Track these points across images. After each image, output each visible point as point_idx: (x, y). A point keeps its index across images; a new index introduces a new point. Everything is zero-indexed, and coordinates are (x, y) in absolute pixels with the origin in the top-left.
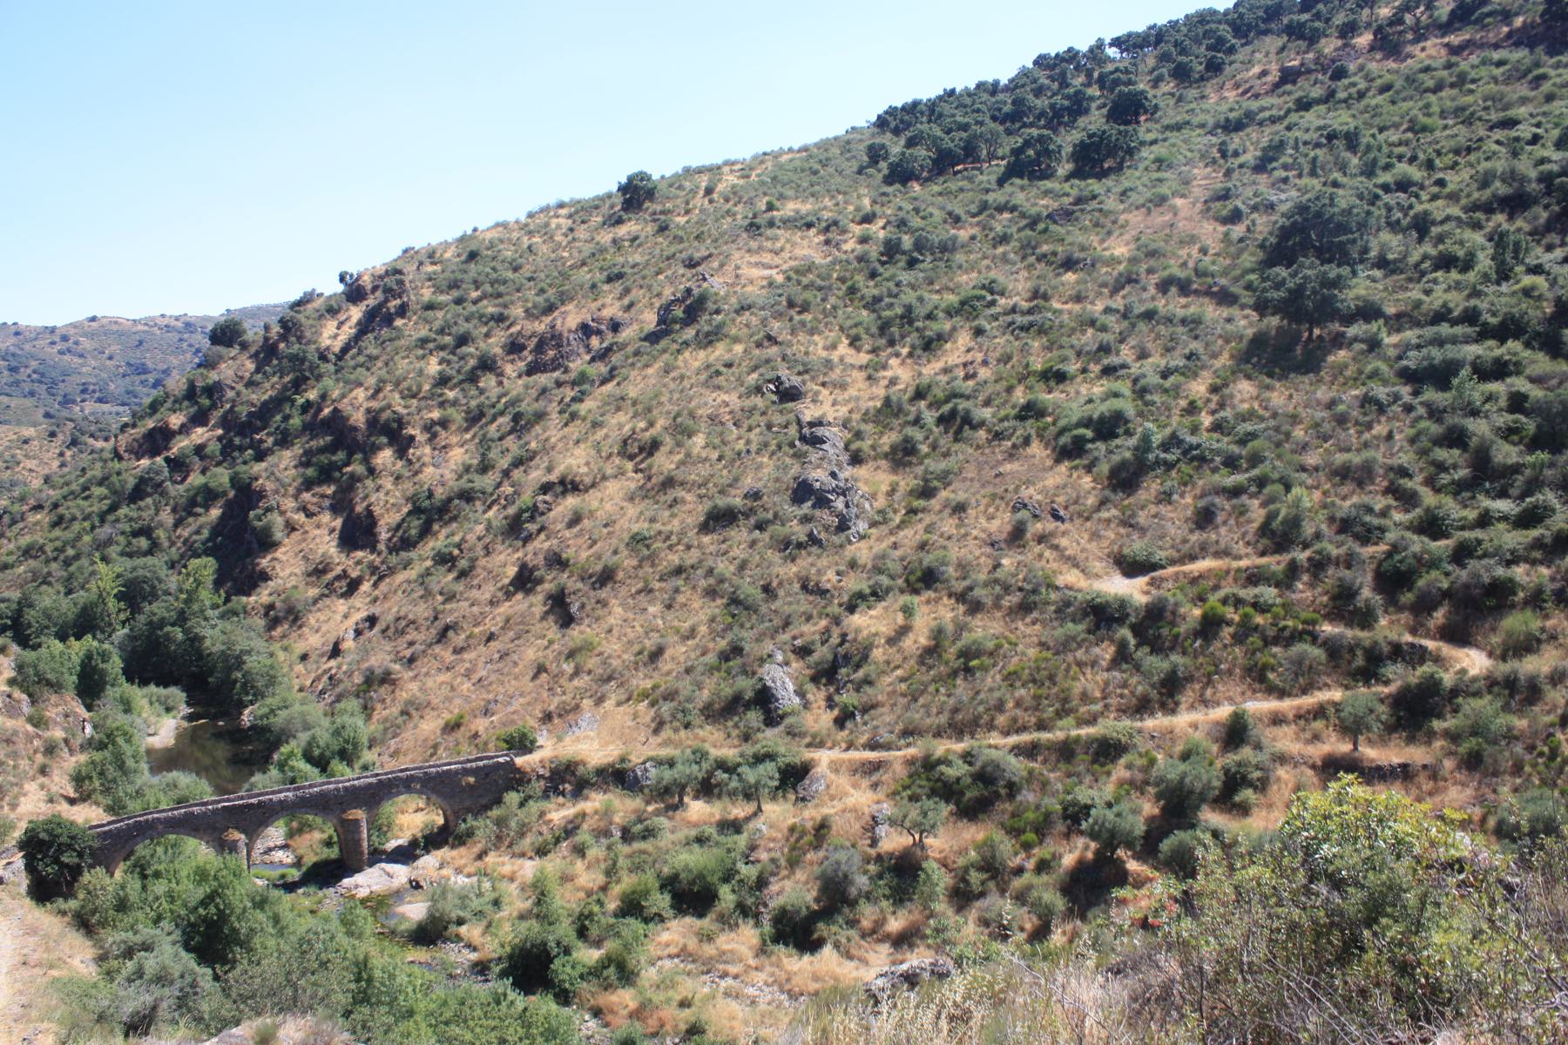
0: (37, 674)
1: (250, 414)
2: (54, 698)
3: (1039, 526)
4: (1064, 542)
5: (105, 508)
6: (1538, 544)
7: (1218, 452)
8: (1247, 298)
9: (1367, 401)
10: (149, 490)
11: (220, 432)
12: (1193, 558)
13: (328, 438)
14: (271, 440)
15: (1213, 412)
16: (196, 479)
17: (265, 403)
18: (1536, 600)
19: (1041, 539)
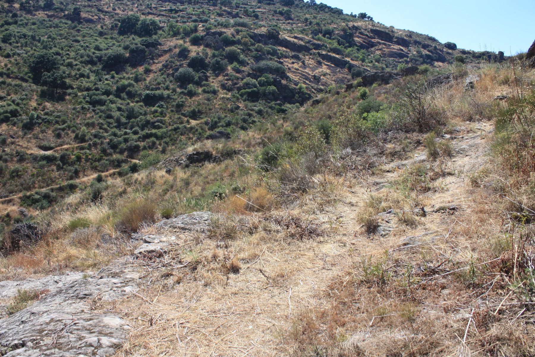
3: (9, 140)
4: (21, 144)
6: (140, 138)
7: (53, 120)
8: (30, 80)
9: (83, 108)
12: (62, 145)
15: (43, 111)
18: (145, 148)
19: (13, 143)
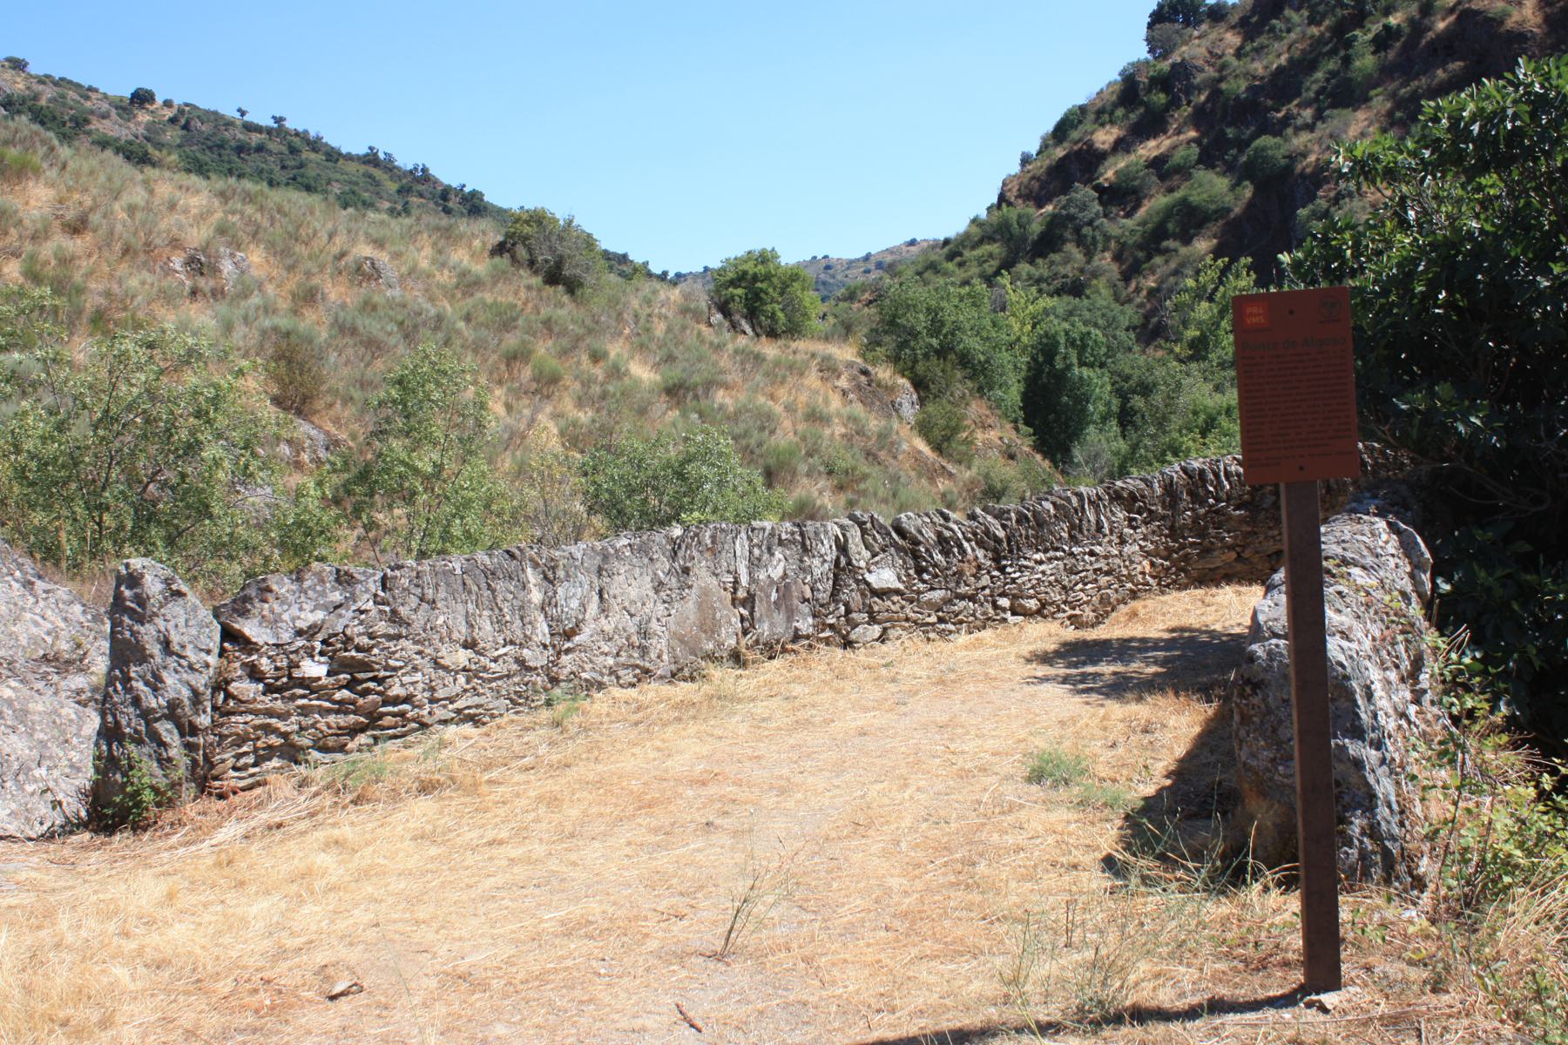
0: (935, 330)
1: (1250, 89)
2: (976, 409)
5: (990, 271)
10: (1068, 235)
11: (1193, 134)
13: (1456, 66)
14: (1308, 114)
16: (1156, 202)
17: (1280, 69)
